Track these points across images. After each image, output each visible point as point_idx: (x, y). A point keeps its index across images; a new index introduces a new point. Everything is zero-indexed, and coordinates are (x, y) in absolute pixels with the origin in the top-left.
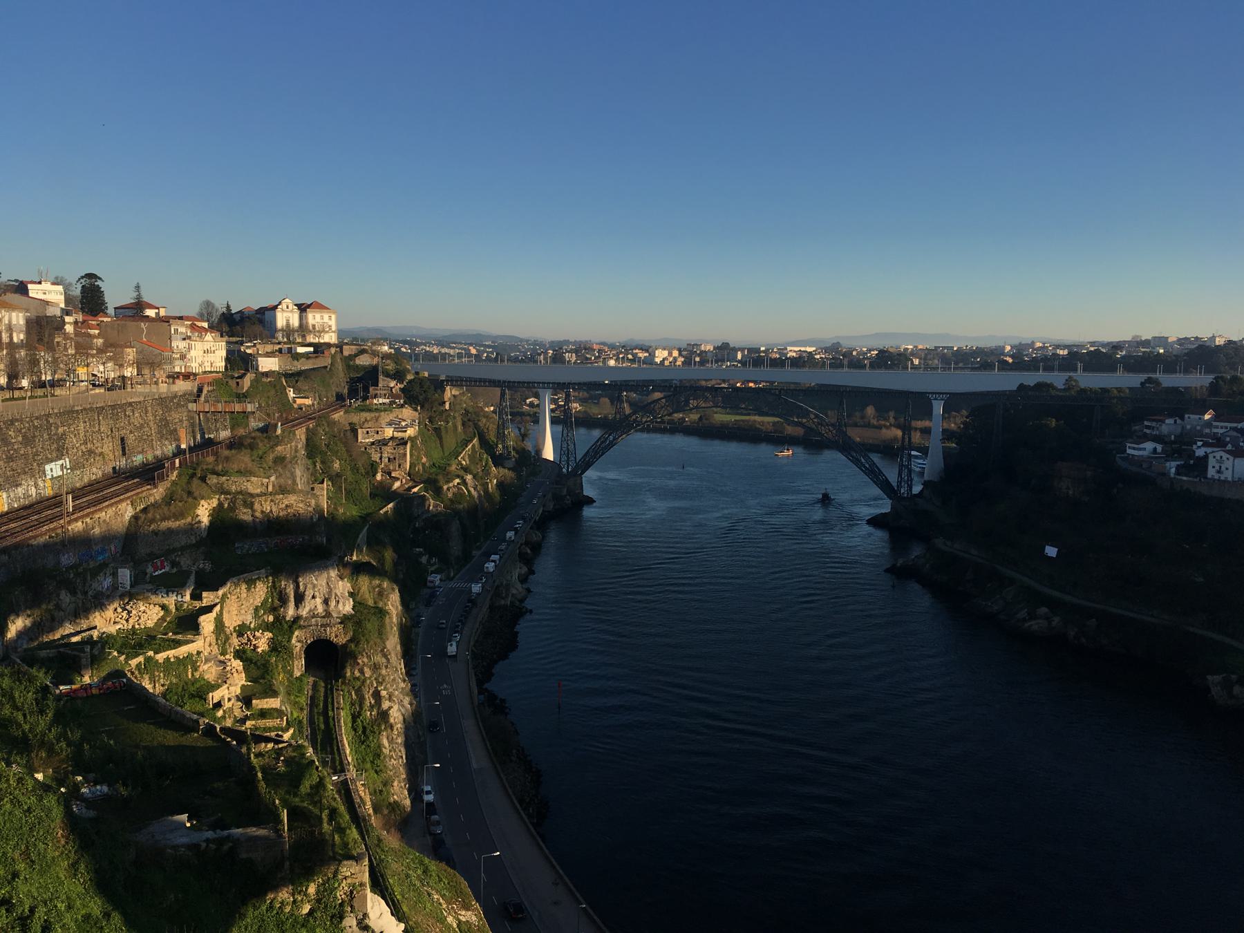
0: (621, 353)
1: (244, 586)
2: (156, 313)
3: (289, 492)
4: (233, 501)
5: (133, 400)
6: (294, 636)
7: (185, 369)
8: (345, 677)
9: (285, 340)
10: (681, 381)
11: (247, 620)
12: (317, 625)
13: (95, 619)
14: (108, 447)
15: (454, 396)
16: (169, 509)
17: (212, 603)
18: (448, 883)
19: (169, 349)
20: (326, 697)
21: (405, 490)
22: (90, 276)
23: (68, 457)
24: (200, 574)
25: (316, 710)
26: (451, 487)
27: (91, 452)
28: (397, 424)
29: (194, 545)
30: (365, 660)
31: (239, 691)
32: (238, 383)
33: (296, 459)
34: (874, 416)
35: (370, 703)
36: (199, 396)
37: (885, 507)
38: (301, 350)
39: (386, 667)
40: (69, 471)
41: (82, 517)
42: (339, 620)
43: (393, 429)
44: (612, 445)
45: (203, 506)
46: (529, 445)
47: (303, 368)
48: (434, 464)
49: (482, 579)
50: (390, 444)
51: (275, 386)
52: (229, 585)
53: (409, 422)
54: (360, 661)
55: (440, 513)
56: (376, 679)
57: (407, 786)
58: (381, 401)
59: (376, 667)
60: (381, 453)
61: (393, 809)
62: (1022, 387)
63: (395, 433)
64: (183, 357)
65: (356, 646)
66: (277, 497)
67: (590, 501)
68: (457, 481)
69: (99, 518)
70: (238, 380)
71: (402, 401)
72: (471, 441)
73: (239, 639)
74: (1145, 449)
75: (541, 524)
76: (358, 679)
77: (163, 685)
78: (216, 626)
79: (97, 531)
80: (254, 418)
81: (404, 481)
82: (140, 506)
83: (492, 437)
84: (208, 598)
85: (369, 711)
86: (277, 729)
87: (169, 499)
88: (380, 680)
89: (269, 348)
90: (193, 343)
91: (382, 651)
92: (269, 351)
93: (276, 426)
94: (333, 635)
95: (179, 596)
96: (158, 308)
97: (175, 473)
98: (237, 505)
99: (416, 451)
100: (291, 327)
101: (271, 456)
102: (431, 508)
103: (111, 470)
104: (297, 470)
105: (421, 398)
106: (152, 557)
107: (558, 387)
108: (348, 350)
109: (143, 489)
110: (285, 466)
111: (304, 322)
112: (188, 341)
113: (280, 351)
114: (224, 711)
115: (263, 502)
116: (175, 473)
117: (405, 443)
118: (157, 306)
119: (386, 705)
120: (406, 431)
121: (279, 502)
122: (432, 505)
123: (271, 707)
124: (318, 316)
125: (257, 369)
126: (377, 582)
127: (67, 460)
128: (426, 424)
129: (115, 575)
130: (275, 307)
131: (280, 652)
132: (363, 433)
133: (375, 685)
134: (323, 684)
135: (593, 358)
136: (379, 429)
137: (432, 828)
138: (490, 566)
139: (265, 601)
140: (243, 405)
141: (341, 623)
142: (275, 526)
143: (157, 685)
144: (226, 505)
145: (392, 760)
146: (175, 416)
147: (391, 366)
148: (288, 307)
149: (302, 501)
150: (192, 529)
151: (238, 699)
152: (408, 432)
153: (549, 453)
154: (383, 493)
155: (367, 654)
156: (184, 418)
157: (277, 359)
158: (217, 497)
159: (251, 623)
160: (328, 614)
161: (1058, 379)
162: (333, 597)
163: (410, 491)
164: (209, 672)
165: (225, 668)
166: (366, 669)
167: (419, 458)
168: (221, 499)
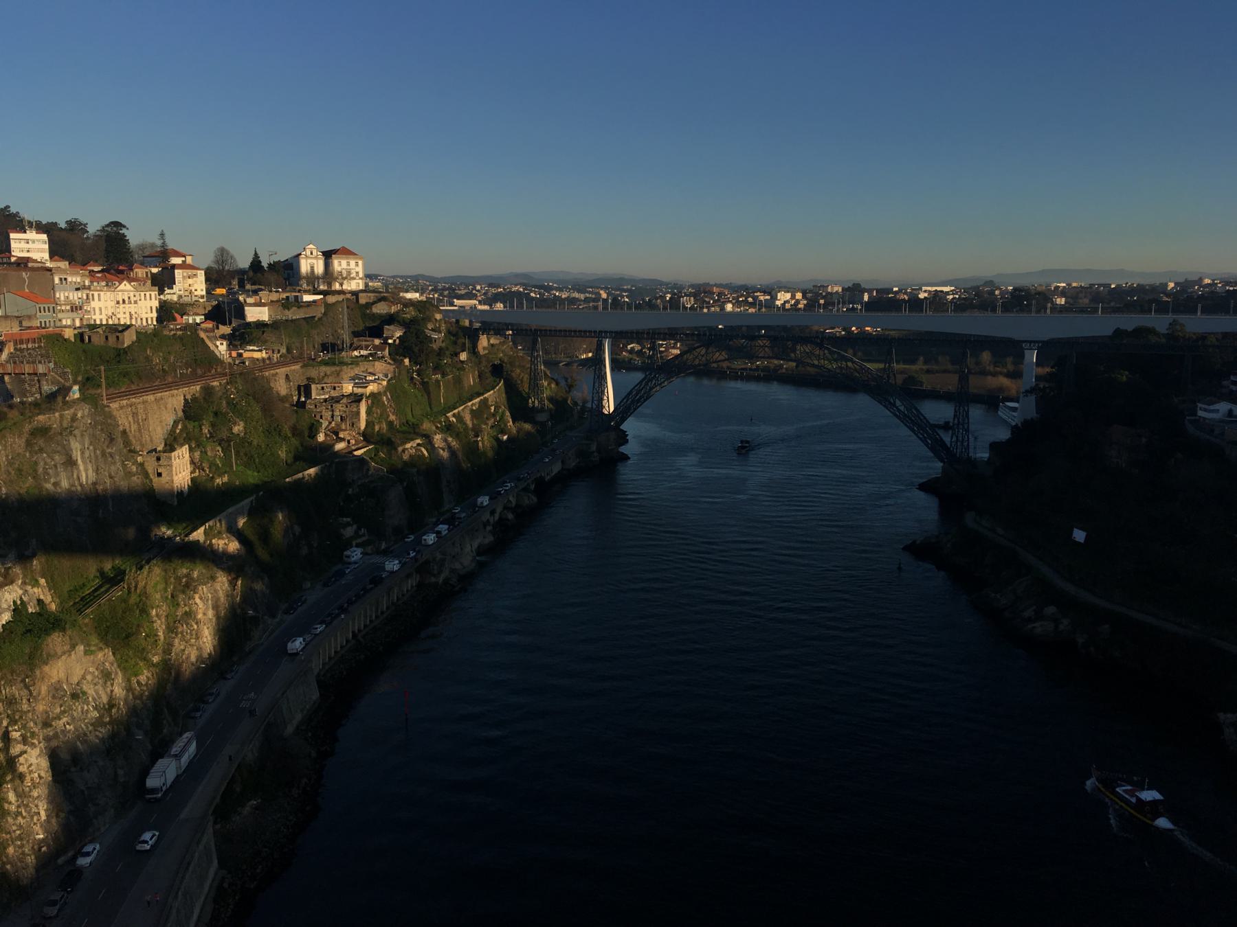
0: (742, 296)
2: (183, 261)
15: (492, 345)
19: (52, 300)
22: (117, 224)
26: (407, 449)
28: (362, 379)
32: (118, 337)
34: (990, 362)
43: (352, 385)
47: (294, 318)
49: (409, 554)
50: (345, 400)
60: (333, 411)
62: (1118, 333)
63: (355, 389)
80: (47, 380)
81: (353, 442)
83: (525, 388)
90: (96, 294)
91: (23, 681)
92: (275, 299)
93: (70, 389)
96: (184, 256)
101: (27, 428)
104: (72, 443)
105: (416, 349)
107: (620, 337)
108: (363, 300)
119: (16, 749)
120: (366, 387)
124: (344, 263)
126: (185, 571)
132: (317, 388)
135: (711, 302)
136: (336, 385)
140: (34, 367)
145: (20, 818)
148: (312, 253)
154: (321, 455)
157: (267, 308)
161: (1159, 323)
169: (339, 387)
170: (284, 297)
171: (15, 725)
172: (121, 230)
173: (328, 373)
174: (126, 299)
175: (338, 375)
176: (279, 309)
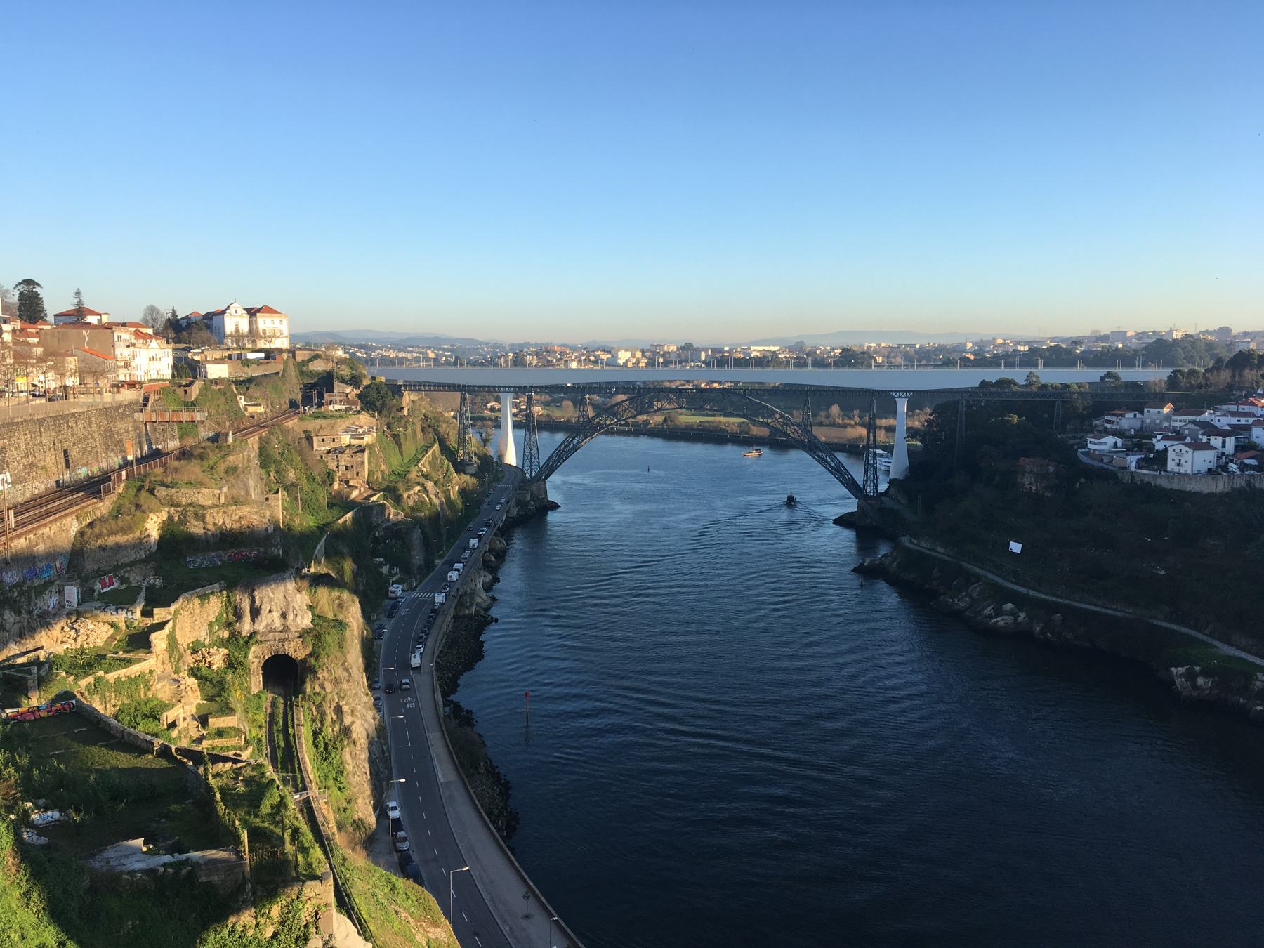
0: (583, 354)
1: (197, 601)
3: (242, 503)
4: (184, 514)
5: (76, 411)
6: (251, 651)
7: (130, 378)
8: (304, 693)
9: (235, 346)
10: (644, 382)
11: (201, 636)
12: (275, 640)
13: (42, 639)
14: (51, 460)
15: (413, 401)
16: (116, 523)
17: (164, 620)
18: (417, 901)
19: (113, 357)
20: (285, 714)
21: (364, 499)
22: (28, 282)
23: (9, 471)
24: (150, 589)
25: (275, 728)
27: (33, 465)
28: (354, 431)
29: (142, 561)
30: (326, 675)
31: (194, 711)
32: (186, 391)
33: (249, 469)
35: (332, 718)
36: (145, 405)
37: (852, 505)
38: (251, 356)
39: (348, 681)
40: (10, 486)
41: (25, 533)
42: (297, 635)
43: (349, 436)
44: (575, 449)
45: (152, 519)
46: (491, 451)
47: (254, 375)
48: (393, 472)
49: (445, 589)
50: (347, 451)
51: (225, 394)
52: (181, 600)
53: (367, 428)
54: (320, 676)
55: (400, 522)
56: (337, 694)
57: (372, 802)
58: (337, 407)
59: (337, 682)
60: (338, 461)
61: (358, 826)
62: (984, 384)
63: (352, 440)
64: (127, 365)
65: (316, 661)
66: (230, 508)
67: (555, 506)
68: (418, 488)
69: (43, 534)
70: (185, 388)
71: (358, 407)
72: (430, 447)
73: (194, 656)
74: (1105, 443)
75: (506, 531)
76: (318, 694)
77: (114, 706)
78: (169, 643)
79: (41, 548)
80: (204, 427)
81: (362, 489)
82: (86, 520)
83: (452, 442)
84: (159, 614)
85: (330, 726)
86: (235, 748)
87: (117, 513)
88: (342, 695)
89: (218, 354)
90: (137, 350)
92: (218, 357)
93: (226, 435)
94: (292, 650)
95: (130, 613)
96: (100, 315)
97: (122, 486)
98: (188, 517)
99: (373, 458)
100: (241, 332)
101: (222, 467)
102: (391, 516)
103: (55, 485)
105: (378, 404)
106: (99, 573)
107: (520, 390)
108: (300, 356)
109: (89, 503)
110: (238, 476)
111: (254, 326)
112: (132, 348)
113: (230, 357)
114: (179, 731)
115: (215, 515)
116: (122, 486)
117: (363, 451)
118: (101, 313)
119: (347, 720)
120: (363, 438)
121: (232, 514)
122: (392, 513)
123: (229, 725)
125: (206, 377)
127: (8, 474)
128: (384, 431)
129: (61, 592)
130: (223, 312)
131: (236, 668)
133: (337, 700)
134: (282, 701)
135: (555, 360)
136: (335, 437)
137: (399, 845)
138: (453, 575)
139: (220, 616)
141: (300, 637)
142: (228, 539)
143: (108, 706)
144: (176, 519)
145: (356, 776)
146: (120, 426)
147: (346, 372)
148: (236, 312)
149: (256, 512)
150: (140, 544)
151: (194, 718)
152: (366, 439)
153: (511, 458)
154: (341, 503)
155: (327, 668)
156: (130, 429)
157: (226, 365)
158: (167, 509)
159: (205, 639)
160: (286, 629)
161: (1019, 376)
162: (291, 610)
163: (369, 500)
164: (162, 691)
165: (179, 686)
166: (327, 684)
167: (378, 466)
168: (171, 512)
169: (337, 439)
170: (227, 355)
171: (343, 700)
172: (35, 287)
173: (324, 426)
174: (155, 357)
175: (333, 427)
176: (239, 366)
